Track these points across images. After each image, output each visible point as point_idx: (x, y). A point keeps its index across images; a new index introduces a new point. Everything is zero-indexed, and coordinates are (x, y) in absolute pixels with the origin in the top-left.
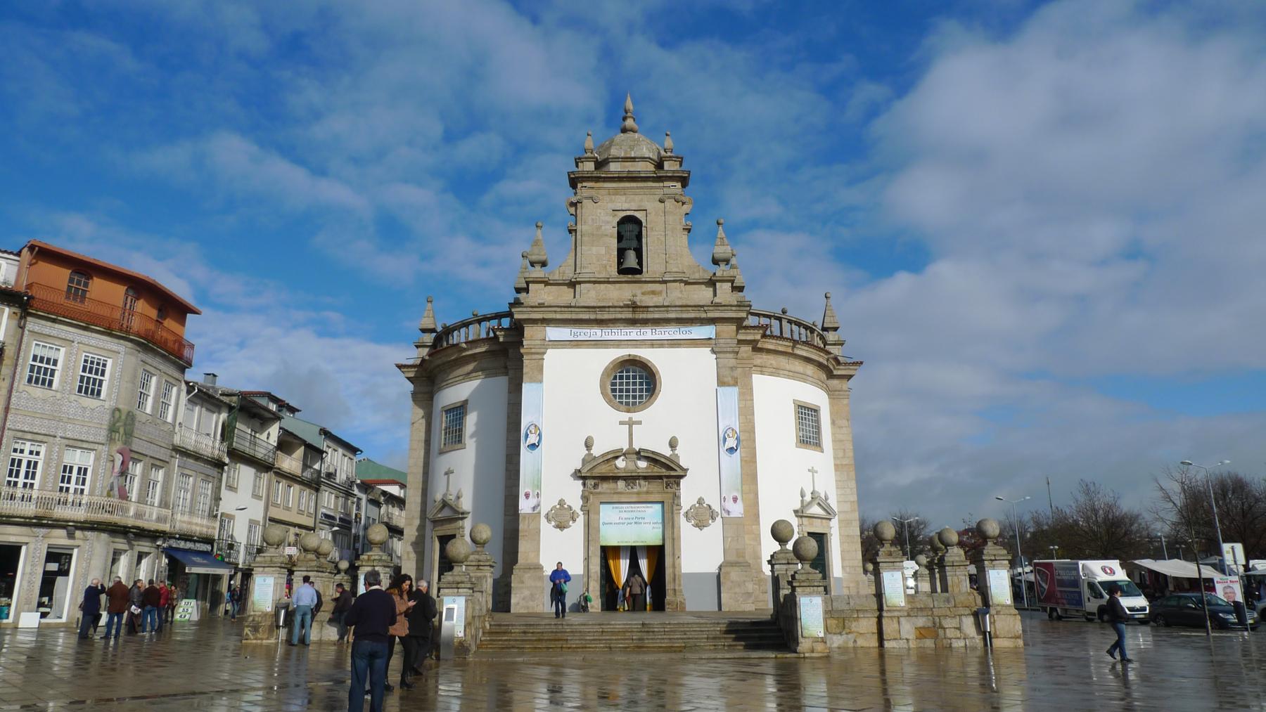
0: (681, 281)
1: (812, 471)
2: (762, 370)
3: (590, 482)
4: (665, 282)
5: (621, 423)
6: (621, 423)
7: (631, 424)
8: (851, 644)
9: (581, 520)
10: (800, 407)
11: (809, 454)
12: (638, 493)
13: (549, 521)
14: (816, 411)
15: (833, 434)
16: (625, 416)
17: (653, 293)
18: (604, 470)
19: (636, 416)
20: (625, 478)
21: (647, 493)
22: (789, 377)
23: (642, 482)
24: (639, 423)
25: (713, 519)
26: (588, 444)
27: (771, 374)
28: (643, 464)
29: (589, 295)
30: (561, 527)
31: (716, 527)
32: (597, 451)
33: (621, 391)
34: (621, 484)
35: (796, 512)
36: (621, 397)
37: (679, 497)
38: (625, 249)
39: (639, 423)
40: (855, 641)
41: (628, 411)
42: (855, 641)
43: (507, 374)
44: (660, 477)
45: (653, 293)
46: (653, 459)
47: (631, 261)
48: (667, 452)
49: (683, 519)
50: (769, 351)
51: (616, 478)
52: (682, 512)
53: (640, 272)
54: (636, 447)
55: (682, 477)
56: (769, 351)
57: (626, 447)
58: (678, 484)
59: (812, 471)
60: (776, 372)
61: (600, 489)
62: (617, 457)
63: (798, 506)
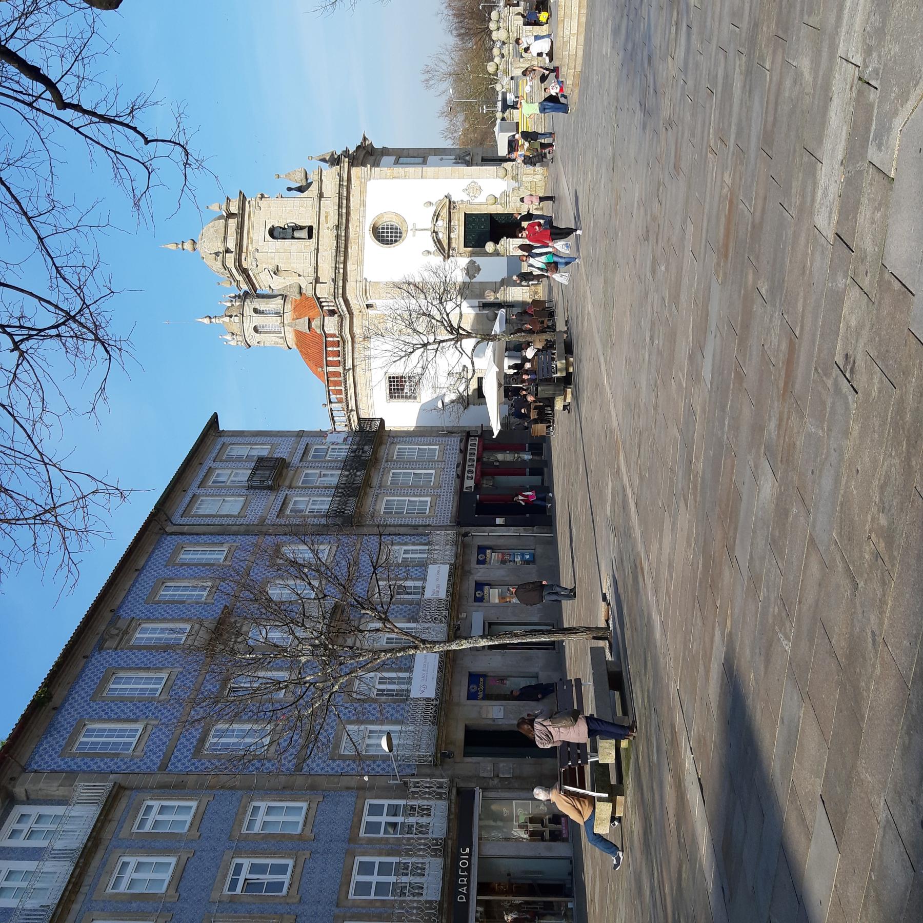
5: (414, 235)
6: (414, 235)
7: (415, 229)
16: (410, 233)
19: (410, 227)
25: (476, 183)
30: (478, 269)
31: (481, 182)
34: (452, 236)
36: (396, 237)
45: (326, 217)
46: (437, 216)
48: (433, 209)
49: (477, 201)
51: (449, 239)
53: (310, 229)
54: (429, 225)
57: (429, 233)
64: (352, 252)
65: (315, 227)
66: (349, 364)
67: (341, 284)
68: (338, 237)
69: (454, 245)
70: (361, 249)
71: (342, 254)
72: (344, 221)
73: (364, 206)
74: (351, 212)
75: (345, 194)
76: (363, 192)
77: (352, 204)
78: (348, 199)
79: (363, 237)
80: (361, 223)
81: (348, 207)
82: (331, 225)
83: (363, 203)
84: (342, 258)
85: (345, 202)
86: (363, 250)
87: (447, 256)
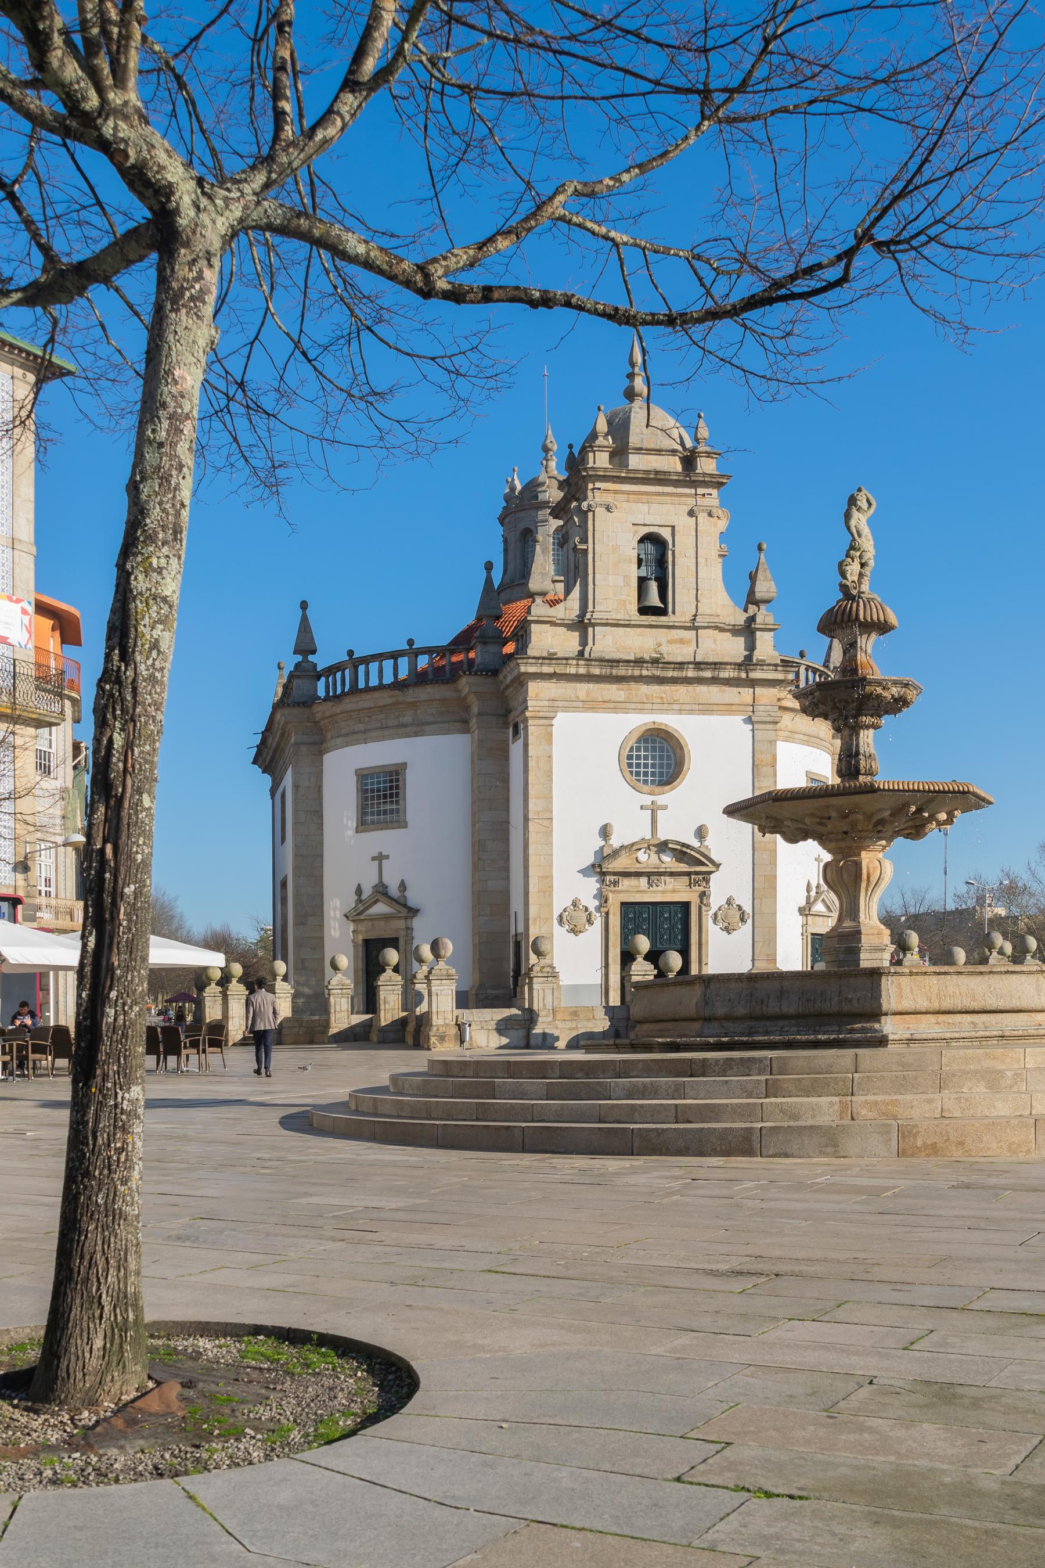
3: (608, 878)
9: (598, 922)
16: (647, 800)
17: (681, 641)
19: (661, 800)
20: (648, 875)
24: (665, 808)
26: (605, 832)
28: (667, 858)
32: (615, 842)
33: (638, 765)
34: (644, 881)
39: (665, 808)
43: (467, 730)
45: (681, 641)
46: (682, 853)
51: (638, 874)
54: (662, 836)
57: (648, 836)
64: (612, 691)
67: (546, 669)
68: (639, 662)
69: (626, 883)
72: (670, 674)
74: (690, 688)
75: (724, 674)
76: (728, 709)
77: (702, 689)
78: (715, 681)
79: (641, 711)
81: (700, 681)
82: (664, 649)
83: (707, 709)
84: (597, 671)
85: (708, 674)
86: (615, 710)
87: (598, 869)
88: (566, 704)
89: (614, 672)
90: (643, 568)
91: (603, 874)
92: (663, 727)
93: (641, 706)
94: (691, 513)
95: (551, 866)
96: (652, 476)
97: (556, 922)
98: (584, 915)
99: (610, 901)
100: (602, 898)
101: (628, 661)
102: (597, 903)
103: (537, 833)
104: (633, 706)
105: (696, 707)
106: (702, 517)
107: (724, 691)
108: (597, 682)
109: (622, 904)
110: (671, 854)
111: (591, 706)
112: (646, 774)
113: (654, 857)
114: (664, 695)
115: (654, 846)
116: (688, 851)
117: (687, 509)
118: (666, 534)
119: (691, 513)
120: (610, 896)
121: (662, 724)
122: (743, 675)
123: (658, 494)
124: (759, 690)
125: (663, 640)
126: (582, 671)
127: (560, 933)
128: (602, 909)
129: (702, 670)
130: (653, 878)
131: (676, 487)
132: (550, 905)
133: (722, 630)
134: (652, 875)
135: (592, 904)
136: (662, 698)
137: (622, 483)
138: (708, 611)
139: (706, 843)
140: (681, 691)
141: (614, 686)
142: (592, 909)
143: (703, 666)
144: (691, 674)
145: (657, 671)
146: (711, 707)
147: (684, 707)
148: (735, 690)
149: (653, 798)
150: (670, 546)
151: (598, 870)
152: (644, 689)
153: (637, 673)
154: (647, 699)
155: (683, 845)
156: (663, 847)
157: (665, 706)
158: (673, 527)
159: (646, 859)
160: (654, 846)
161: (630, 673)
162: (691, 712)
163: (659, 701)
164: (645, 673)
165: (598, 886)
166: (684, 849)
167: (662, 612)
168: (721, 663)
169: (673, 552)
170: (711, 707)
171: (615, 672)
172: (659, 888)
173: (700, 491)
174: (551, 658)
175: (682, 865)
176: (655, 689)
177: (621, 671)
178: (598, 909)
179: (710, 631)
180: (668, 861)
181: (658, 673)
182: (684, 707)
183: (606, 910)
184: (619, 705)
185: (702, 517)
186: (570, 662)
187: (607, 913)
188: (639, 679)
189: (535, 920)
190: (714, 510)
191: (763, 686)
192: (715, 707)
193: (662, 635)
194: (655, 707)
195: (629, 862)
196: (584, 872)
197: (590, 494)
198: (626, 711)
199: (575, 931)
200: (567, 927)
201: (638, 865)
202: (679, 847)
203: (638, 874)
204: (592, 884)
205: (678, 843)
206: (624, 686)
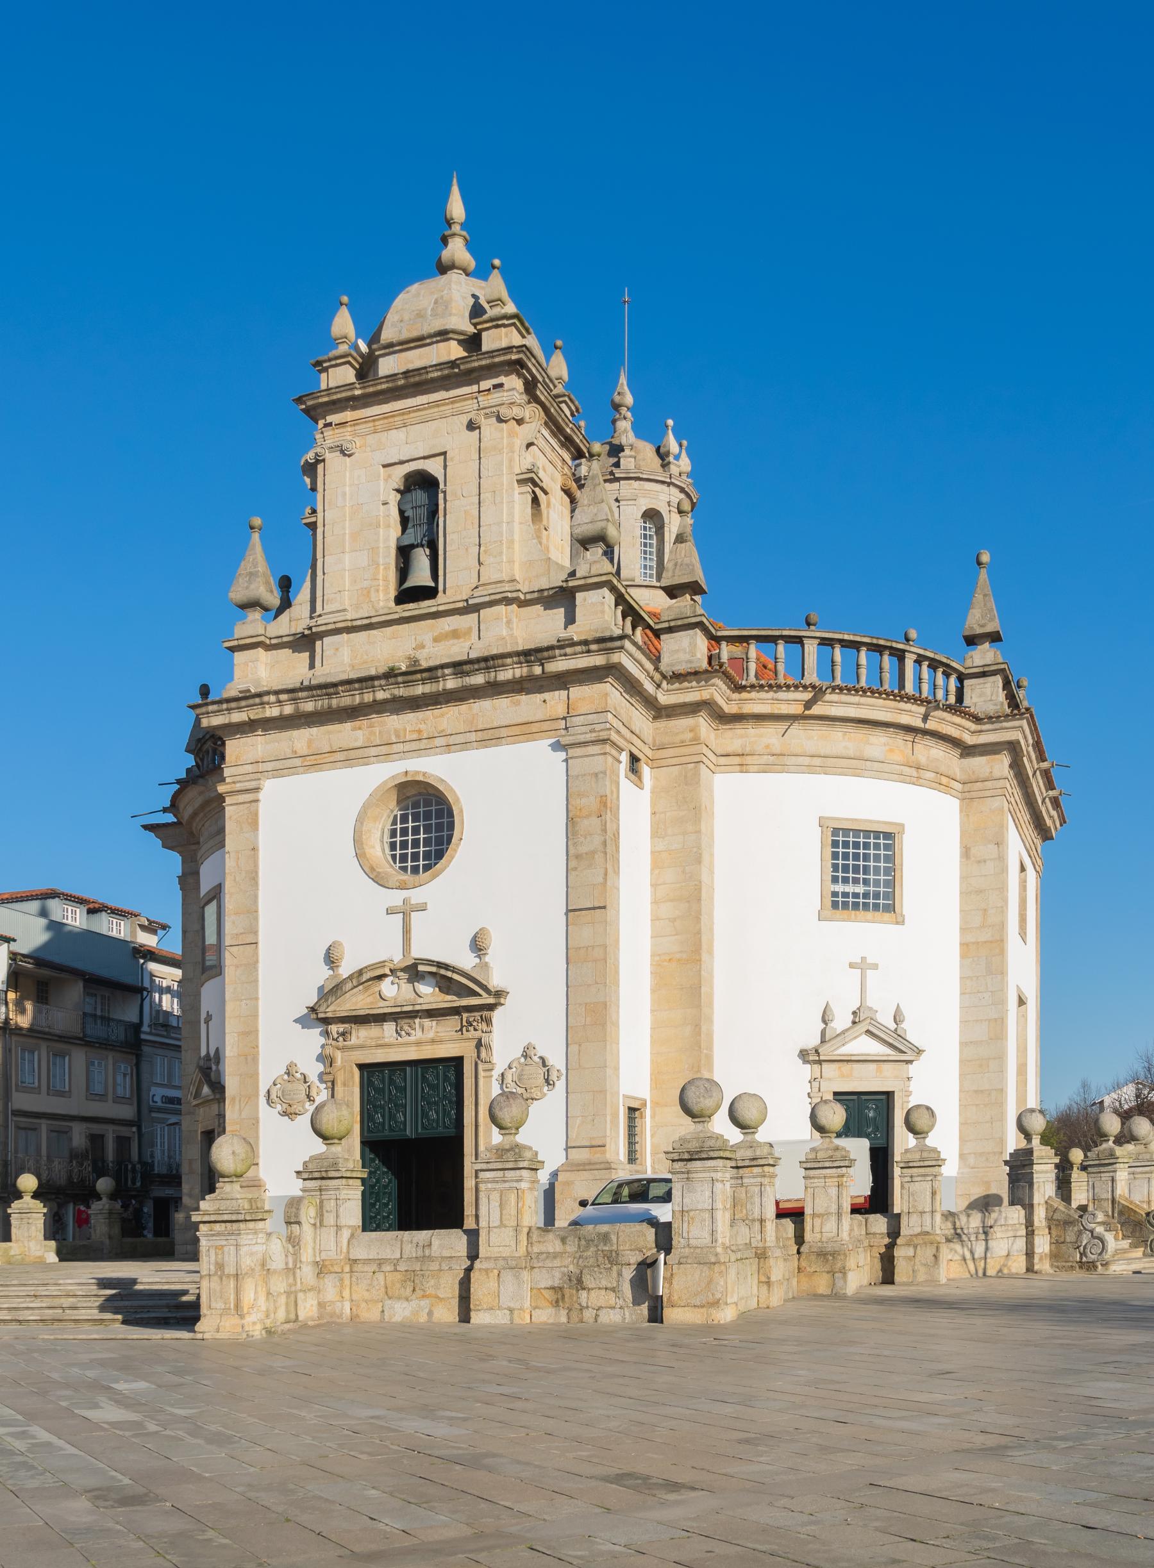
0: (508, 601)
1: (862, 966)
2: (741, 761)
3: (334, 1029)
4: (476, 608)
8: (423, 1318)
10: (835, 832)
11: (863, 934)
12: (418, 1043)
13: (269, 1101)
14: (888, 836)
15: (964, 878)
16: (396, 898)
17: (455, 634)
18: (357, 1002)
19: (416, 896)
20: (395, 1017)
21: (433, 1041)
22: (810, 769)
23: (427, 1022)
24: (422, 908)
27: (766, 769)
29: (341, 658)
32: (345, 970)
34: (389, 1028)
35: (803, 1054)
37: (489, 1047)
38: (412, 547)
39: (422, 908)
40: (430, 1313)
41: (402, 887)
42: (430, 1313)
44: (456, 1011)
45: (455, 634)
46: (444, 977)
47: (421, 576)
48: (466, 961)
50: (760, 718)
51: (379, 1019)
52: (496, 1074)
54: (419, 951)
55: (491, 1007)
56: (760, 718)
58: (489, 1022)
59: (862, 966)
60: (777, 762)
61: (353, 1040)
62: (381, 977)
63: (814, 1041)
65: (426, 606)
66: (834, 705)
69: (361, 1035)
70: (350, 757)
71: (322, 704)
72: (420, 690)
73: (484, 743)
74: (464, 708)
75: (504, 675)
76: (525, 731)
78: (495, 689)
80: (424, 744)
81: (474, 693)
83: (490, 737)
84: (309, 706)
85: (479, 679)
86: (348, 762)
87: (316, 1017)
88: (279, 765)
89: (334, 702)
90: (410, 531)
91: (326, 1021)
92: (421, 778)
93: (386, 750)
94: (471, 426)
95: (255, 1016)
96: (401, 382)
97: (262, 1100)
98: (302, 1088)
99: (339, 1062)
100: (326, 1059)
101: (349, 682)
102: (320, 1067)
103: (237, 966)
104: (373, 751)
105: (473, 737)
106: (489, 427)
107: (518, 703)
108: (322, 723)
109: (362, 1067)
110: (433, 981)
111: (314, 762)
112: (415, 857)
113: (406, 988)
114: (423, 727)
115: (403, 970)
116: (449, 974)
117: (465, 419)
118: (434, 467)
119: (471, 426)
120: (339, 1056)
121: (417, 773)
122: (537, 670)
123: (437, 404)
124: (576, 691)
125: (427, 638)
126: (288, 710)
127: (268, 1117)
128: (325, 1078)
129: (468, 674)
130: (402, 1022)
131: (447, 390)
132: (254, 1076)
133: (523, 604)
134: (402, 1016)
135: (313, 1070)
136: (419, 731)
137: (366, 405)
138: (495, 577)
139: (487, 959)
140: (450, 717)
141: (348, 726)
142: (313, 1078)
143: (466, 668)
144: (451, 684)
145: (411, 690)
146: (497, 733)
147: (452, 740)
148: (538, 698)
149: (405, 894)
150: (442, 486)
151: (314, 1016)
152: (393, 722)
153: (368, 698)
154: (398, 736)
155: (439, 965)
156: (414, 972)
157: (423, 744)
158: (444, 453)
159: (393, 991)
160: (403, 970)
161: (357, 699)
162: (465, 745)
163: (415, 736)
164: (381, 695)
165: (322, 1040)
166: (443, 972)
167: (429, 593)
168: (494, 657)
169: (445, 492)
170: (497, 733)
171: (333, 705)
172: (412, 1038)
173: (486, 384)
174: (247, 697)
175: (449, 998)
176: (407, 722)
177: (346, 700)
178: (321, 1077)
179: (501, 609)
180: (428, 994)
181: (402, 692)
182: (452, 740)
183: (330, 1078)
184: (353, 754)
185: (489, 427)
186: (266, 699)
187: (333, 1082)
188: (378, 707)
189: (233, 1099)
190: (504, 412)
191: (581, 682)
192: (504, 732)
193: (425, 631)
194: (408, 747)
195: (369, 1000)
196: (303, 1021)
197: (318, 436)
198: (365, 760)
199: (288, 1114)
200: (279, 1107)
201: (382, 1004)
202: (434, 969)
203: (379, 1019)
204: (314, 1038)
205: (430, 962)
206: (363, 722)
